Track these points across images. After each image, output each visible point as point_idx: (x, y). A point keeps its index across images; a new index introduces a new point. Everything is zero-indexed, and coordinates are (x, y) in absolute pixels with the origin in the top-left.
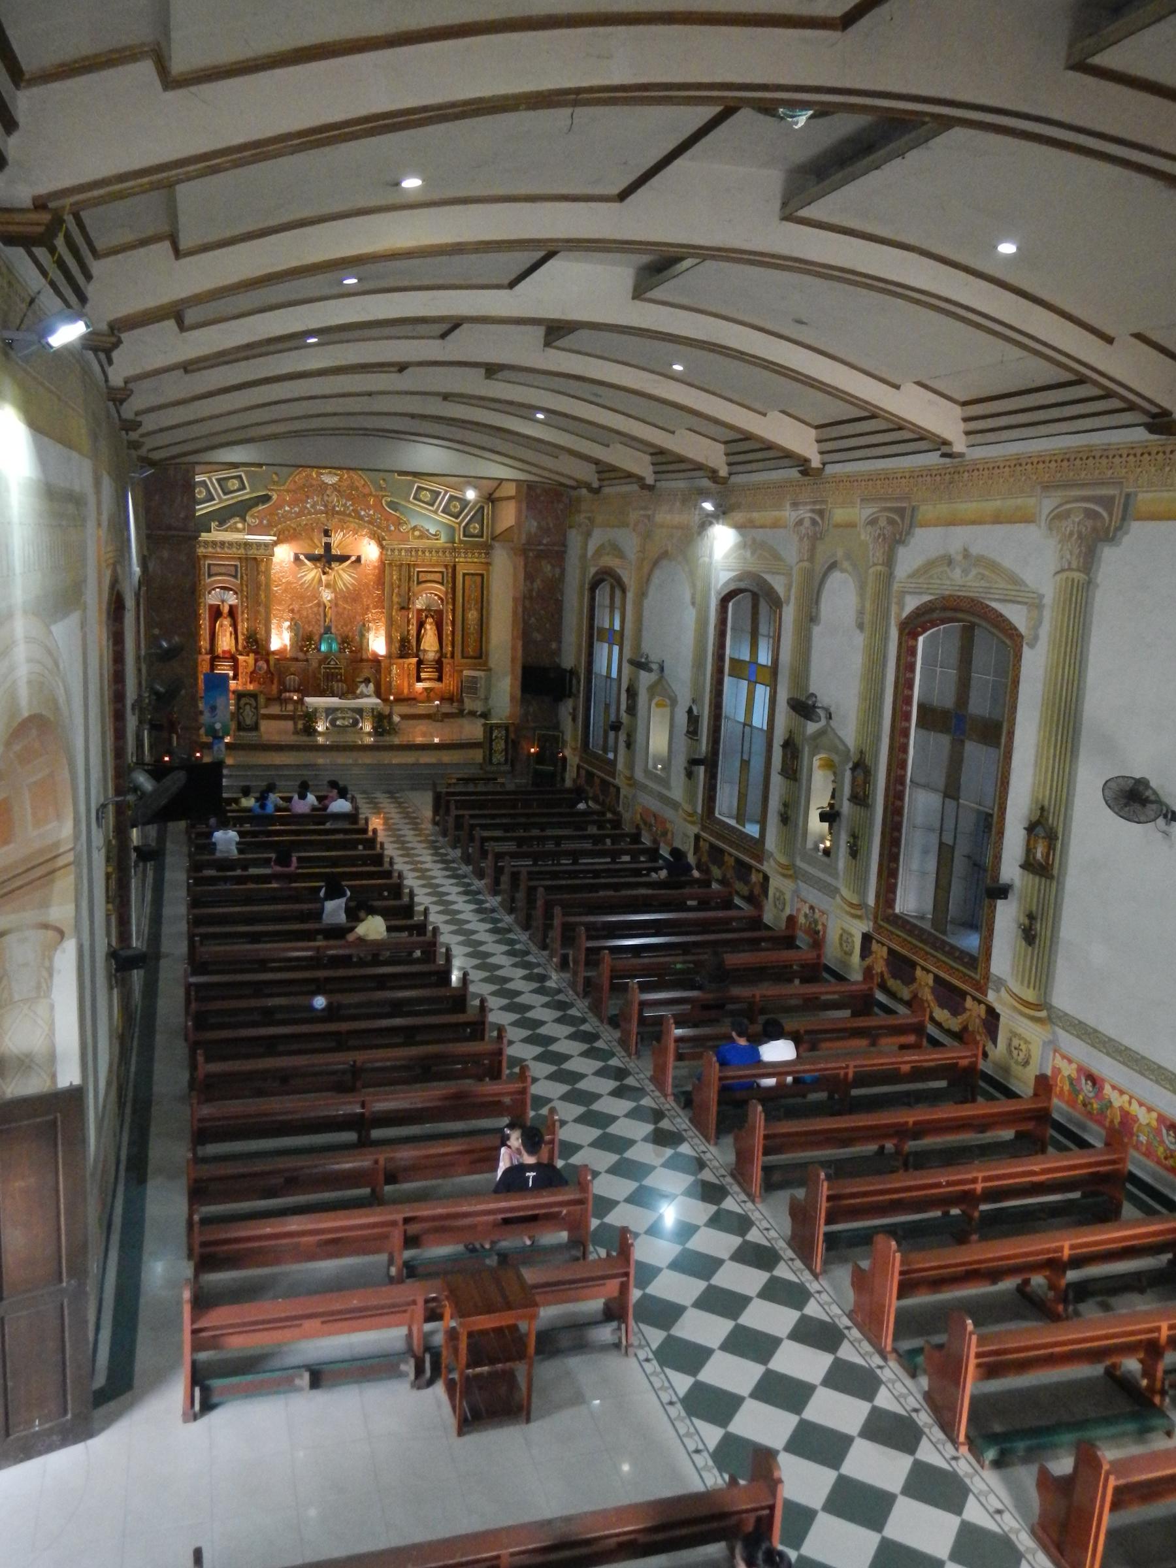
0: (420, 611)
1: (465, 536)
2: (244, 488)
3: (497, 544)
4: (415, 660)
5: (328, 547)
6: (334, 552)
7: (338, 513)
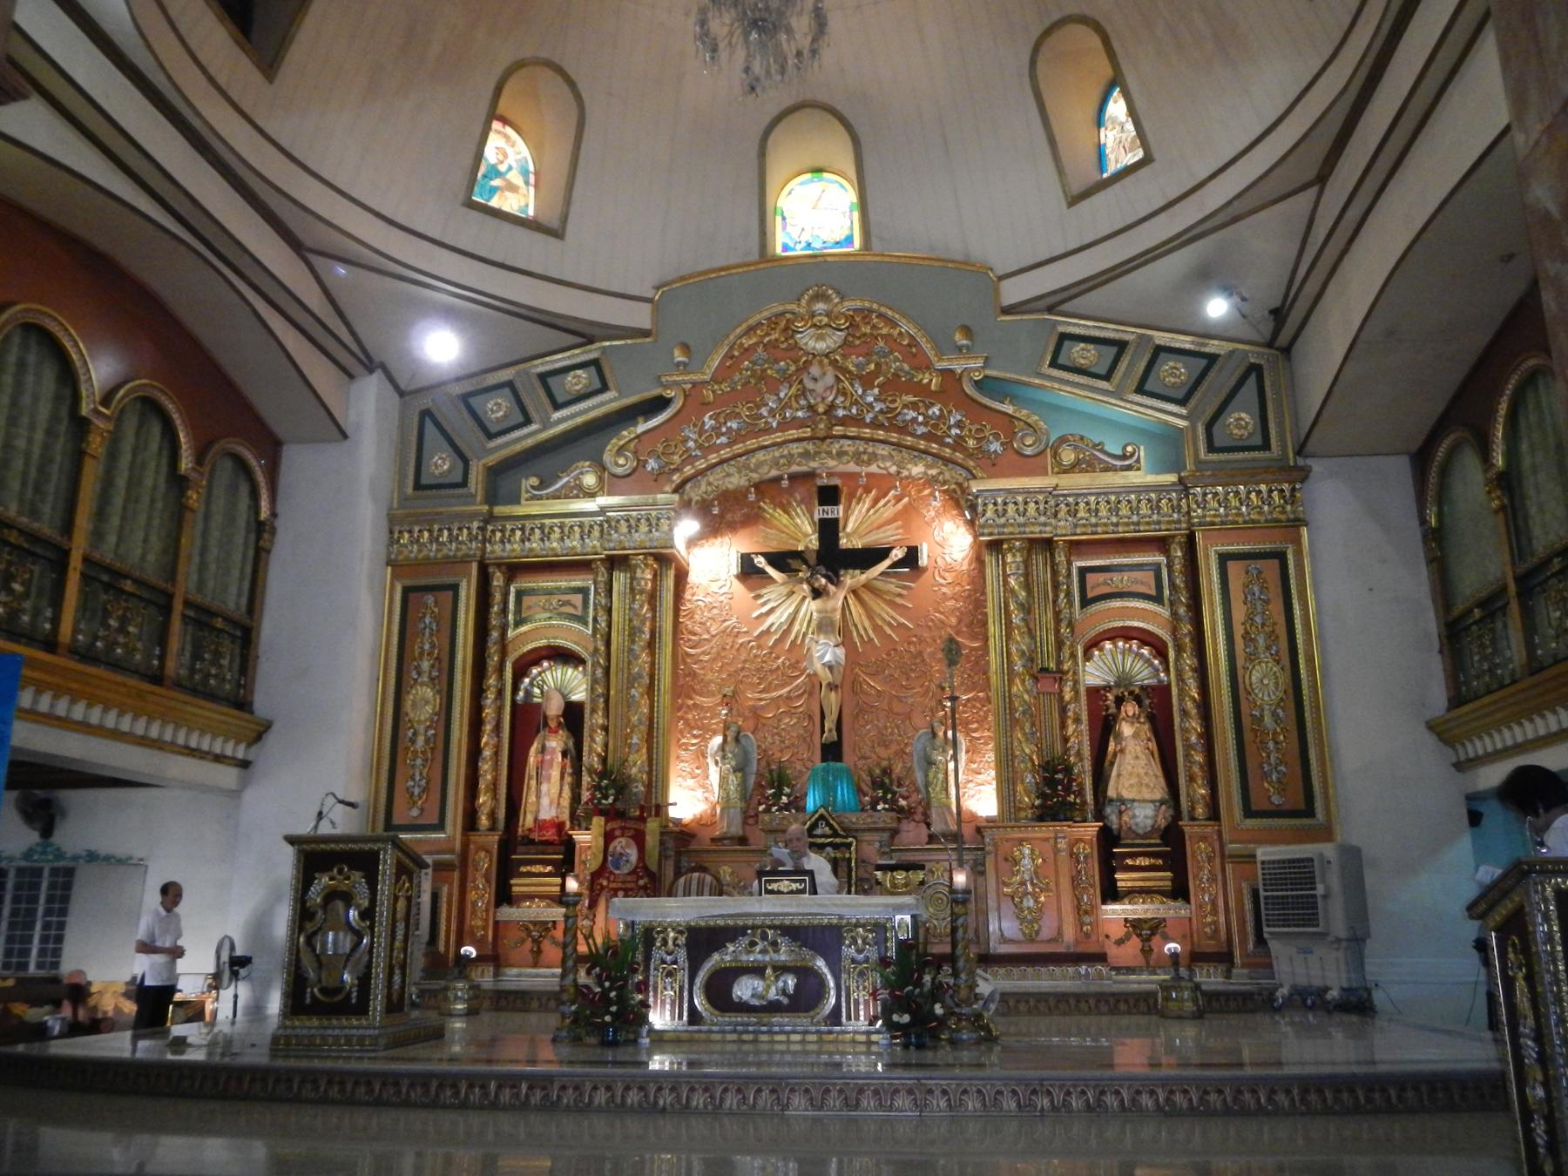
0: (1095, 693)
1: (1211, 448)
2: (605, 388)
3: (1317, 466)
4: (1091, 829)
5: (829, 530)
6: (844, 543)
7: (843, 422)
